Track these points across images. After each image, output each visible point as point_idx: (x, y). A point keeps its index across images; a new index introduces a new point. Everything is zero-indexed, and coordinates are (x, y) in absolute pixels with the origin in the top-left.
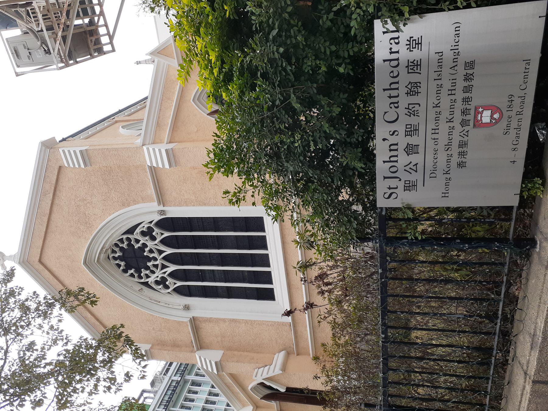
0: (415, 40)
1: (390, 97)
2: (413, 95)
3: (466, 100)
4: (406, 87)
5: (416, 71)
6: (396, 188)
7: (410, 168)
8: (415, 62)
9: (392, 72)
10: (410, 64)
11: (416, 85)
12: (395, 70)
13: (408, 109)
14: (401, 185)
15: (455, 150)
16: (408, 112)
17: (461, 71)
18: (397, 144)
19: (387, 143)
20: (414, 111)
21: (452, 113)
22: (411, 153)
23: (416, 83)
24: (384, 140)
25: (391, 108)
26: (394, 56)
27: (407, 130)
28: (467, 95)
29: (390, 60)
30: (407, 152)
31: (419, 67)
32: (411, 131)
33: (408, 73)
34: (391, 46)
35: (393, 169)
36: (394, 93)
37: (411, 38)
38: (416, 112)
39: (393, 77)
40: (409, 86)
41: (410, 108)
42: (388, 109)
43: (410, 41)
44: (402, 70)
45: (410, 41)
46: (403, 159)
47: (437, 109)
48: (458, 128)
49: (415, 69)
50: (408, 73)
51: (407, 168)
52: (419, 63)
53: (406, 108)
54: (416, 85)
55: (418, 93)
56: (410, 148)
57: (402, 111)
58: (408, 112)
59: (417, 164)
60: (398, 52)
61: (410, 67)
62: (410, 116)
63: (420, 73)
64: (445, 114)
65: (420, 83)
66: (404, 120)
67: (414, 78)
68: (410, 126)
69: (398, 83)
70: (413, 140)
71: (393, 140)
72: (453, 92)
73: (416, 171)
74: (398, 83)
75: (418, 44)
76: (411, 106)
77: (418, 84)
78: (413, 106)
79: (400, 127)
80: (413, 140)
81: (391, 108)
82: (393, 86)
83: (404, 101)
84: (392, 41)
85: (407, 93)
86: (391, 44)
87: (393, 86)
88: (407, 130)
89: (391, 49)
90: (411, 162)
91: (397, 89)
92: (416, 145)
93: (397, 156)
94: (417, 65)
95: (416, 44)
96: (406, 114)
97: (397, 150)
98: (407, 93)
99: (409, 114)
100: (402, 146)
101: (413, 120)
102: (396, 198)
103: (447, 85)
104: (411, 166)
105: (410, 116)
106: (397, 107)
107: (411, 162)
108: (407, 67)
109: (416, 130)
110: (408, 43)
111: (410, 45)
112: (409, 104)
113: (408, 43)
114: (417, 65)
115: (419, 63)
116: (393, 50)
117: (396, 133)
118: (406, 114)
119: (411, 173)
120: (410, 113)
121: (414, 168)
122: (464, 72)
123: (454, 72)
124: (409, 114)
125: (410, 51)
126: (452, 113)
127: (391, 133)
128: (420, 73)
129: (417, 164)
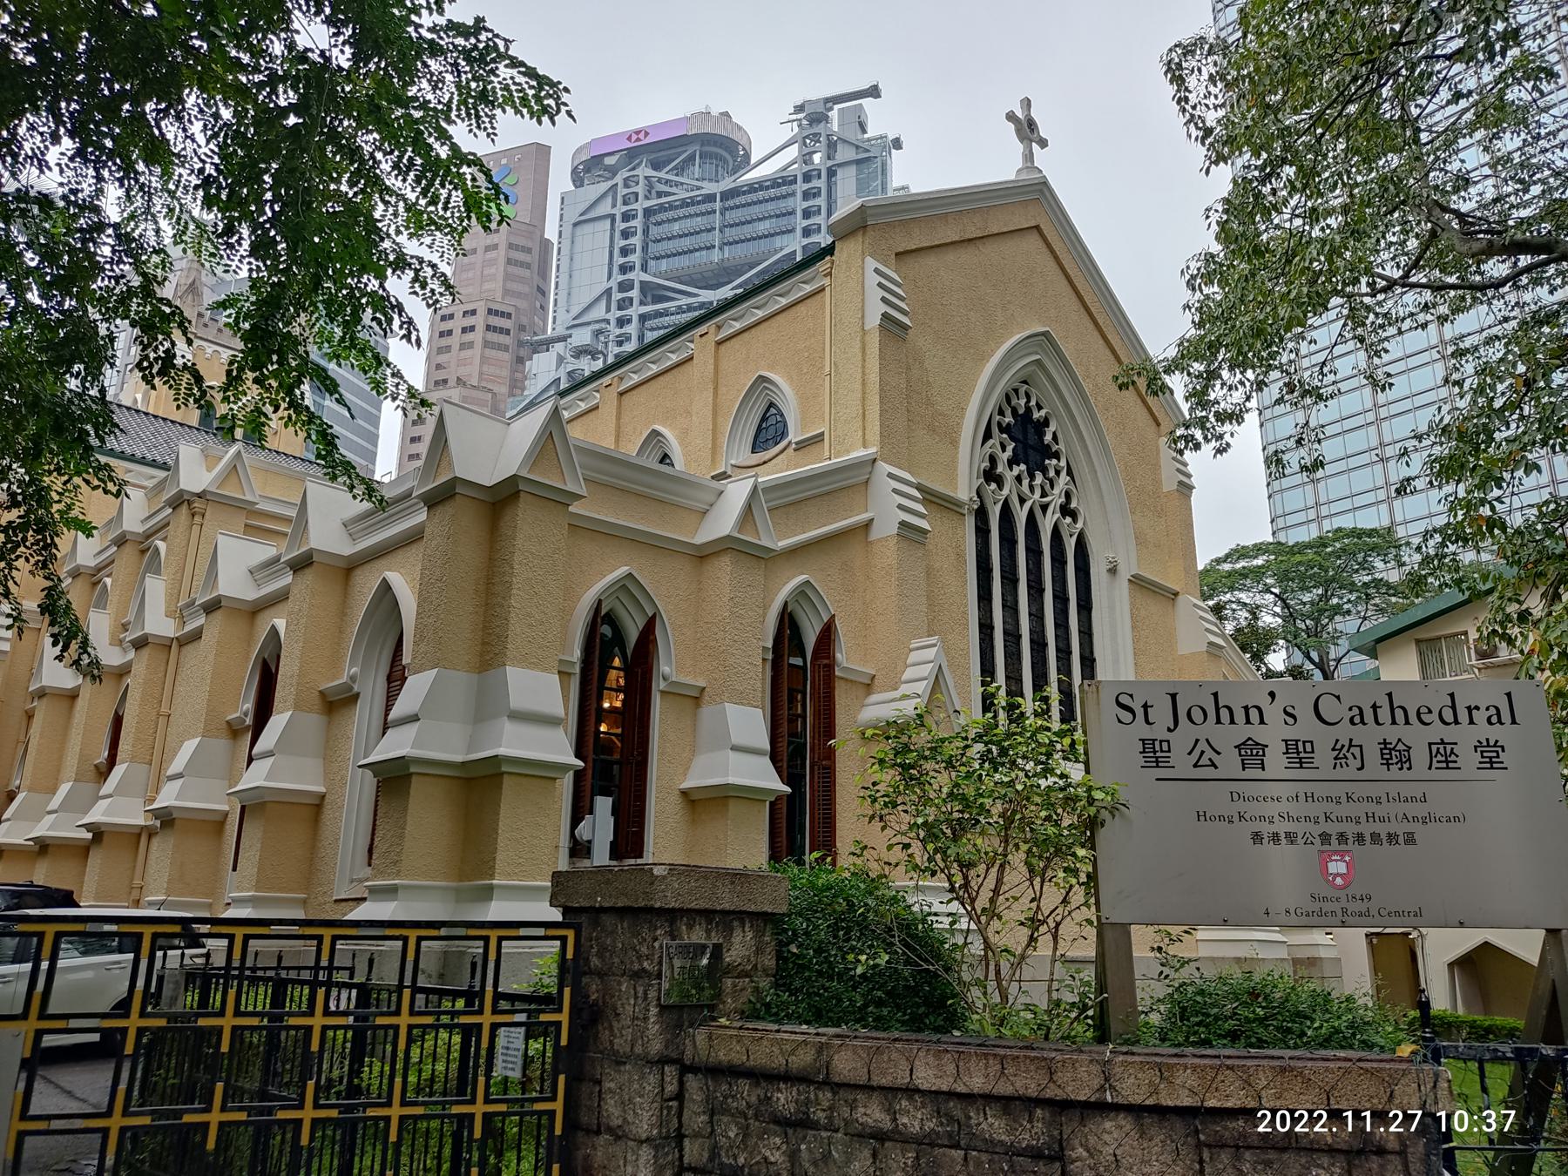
0: (1498, 757)
1: (1375, 707)
2: (1382, 754)
4: (1399, 740)
5: (1435, 760)
6: (1147, 721)
7: (1203, 752)
8: (1453, 758)
9: (1430, 712)
10: (1449, 748)
11: (1405, 761)
12: (1435, 716)
13: (1351, 746)
14: (1159, 732)
16: (1343, 746)
18: (1262, 722)
19: (1264, 701)
20: (1346, 758)
22: (1243, 752)
23: (1409, 759)
24: (1272, 695)
25: (1350, 709)
26: (1463, 716)
27: (1300, 744)
29: (1453, 707)
30: (1244, 744)
31: (1444, 765)
33: (1430, 744)
34: (1483, 709)
35: (1197, 715)
36: (1384, 714)
37: (1502, 747)
38: (1343, 761)
39: (1418, 714)
40: (1401, 746)
41: (1352, 750)
42: (1347, 703)
43: (1495, 746)
44: (1437, 731)
45: (1495, 746)
46: (1228, 736)
47: (1344, 799)
49: (1439, 758)
50: (1430, 744)
51: (1202, 745)
52: (1451, 765)
53: (1351, 740)
55: (1388, 764)
56: (1255, 752)
57: (1344, 732)
58: (1343, 746)
59: (1216, 767)
60: (1471, 722)
61: (1441, 747)
62: (1333, 749)
63: (1430, 768)
65: (1409, 769)
66: (1323, 739)
67: (1420, 756)
68: (1309, 748)
69: (1407, 722)
71: (1273, 713)
73: (1195, 766)
74: (1407, 722)
75: (1491, 763)
76: (1356, 751)
77: (1407, 765)
78: (1358, 756)
79: (1307, 728)
81: (1350, 709)
82: (1399, 714)
83: (1369, 737)
84: (1493, 711)
85: (1385, 742)
86: (1487, 709)
87: (1399, 714)
88: (1300, 744)
89: (1477, 708)
90: (1219, 753)
91: (1394, 722)
92: (1263, 764)
93: (1232, 722)
94: (1447, 762)
95: (1491, 758)
96: (1337, 741)
97: (1248, 722)
98: (1385, 742)
99: (1338, 747)
100: (1257, 733)
101: (1323, 756)
102: (1120, 721)
105: (1333, 749)
106: (1352, 721)
107: (1219, 753)
108: (1442, 742)
109: (1301, 763)
110: (1492, 743)
111: (1488, 746)
112: (1361, 746)
113: (1492, 743)
114: (1447, 762)
115: (1451, 765)
116: (1474, 712)
117: (1290, 720)
118: (1337, 741)
119: (1190, 754)
120: (1341, 750)
121: (1204, 761)
123: (1399, 819)
124: (1338, 747)
125: (1476, 747)
127: (1289, 710)
128: (1430, 768)
129: (1216, 767)
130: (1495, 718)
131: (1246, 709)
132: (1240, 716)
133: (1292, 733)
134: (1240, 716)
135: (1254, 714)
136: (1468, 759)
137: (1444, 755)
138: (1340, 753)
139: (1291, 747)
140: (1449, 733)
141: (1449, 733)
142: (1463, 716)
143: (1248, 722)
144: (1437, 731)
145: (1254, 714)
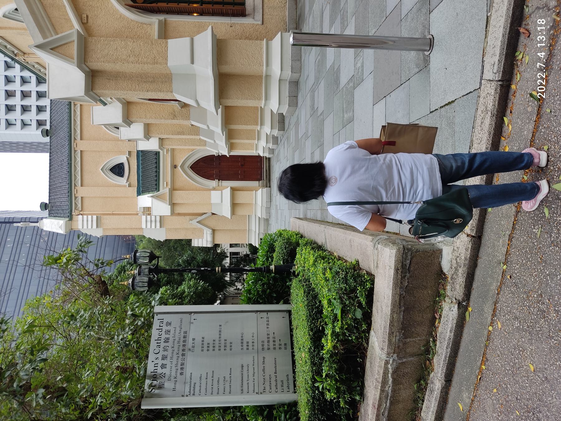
1: (157, 343)
3: (184, 345)
11: (168, 339)
15: (179, 367)
17: (182, 334)
21: (179, 350)
24: (152, 362)
26: (161, 328)
28: (184, 343)
29: (159, 329)
32: (164, 358)
36: (159, 341)
40: (165, 339)
42: (155, 348)
44: (163, 333)
47: (173, 349)
48: (181, 357)
54: (168, 339)
57: (161, 349)
64: (176, 351)
70: (164, 362)
71: (156, 362)
72: (179, 342)
79: (160, 356)
80: (164, 362)
82: (159, 339)
83: (163, 344)
87: (159, 339)
93: (157, 369)
100: (159, 365)
101: (165, 353)
103: (177, 339)
104: (163, 374)
117: (158, 359)
122: (183, 335)
126: (179, 350)
130: (162, 322)
131: (155, 367)
132: (156, 368)
133: (160, 358)
134: (156, 368)
135: (156, 365)
136: (168, 328)
137: (168, 332)
138: (165, 350)
139: (163, 359)
140: (164, 331)
141: (164, 331)
142: (161, 328)
143: (157, 366)
144: (163, 333)
145: (156, 365)
